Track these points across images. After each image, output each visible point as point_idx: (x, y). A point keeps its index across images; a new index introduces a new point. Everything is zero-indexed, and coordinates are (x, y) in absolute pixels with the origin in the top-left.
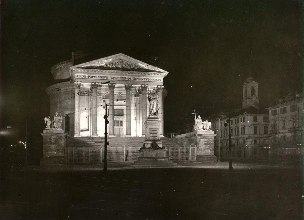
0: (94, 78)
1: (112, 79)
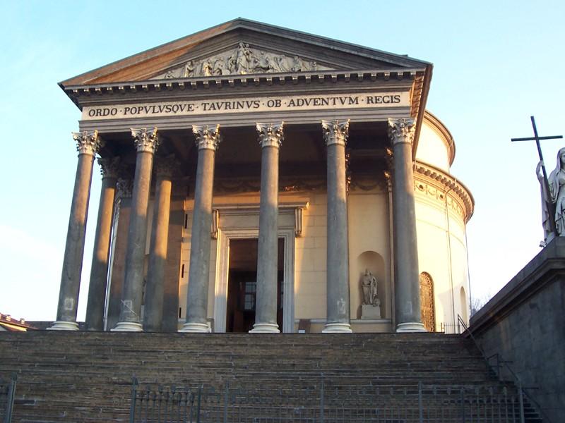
0: (143, 114)
1: (205, 113)
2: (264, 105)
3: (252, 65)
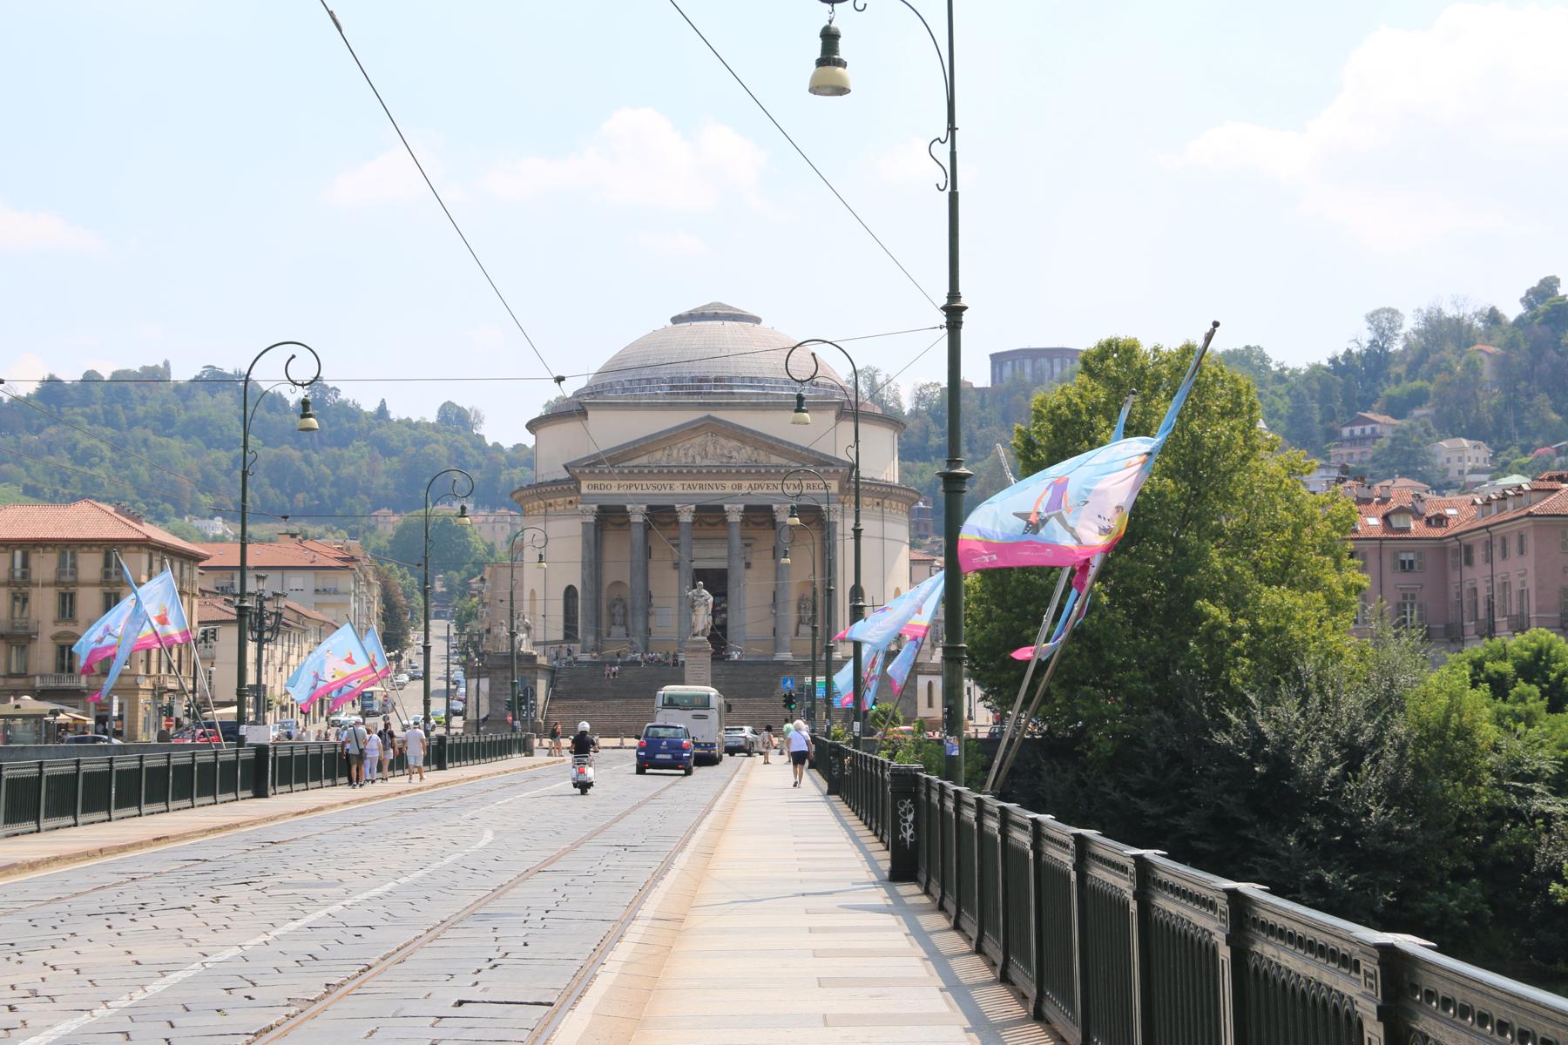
0: (633, 490)
2: (729, 486)
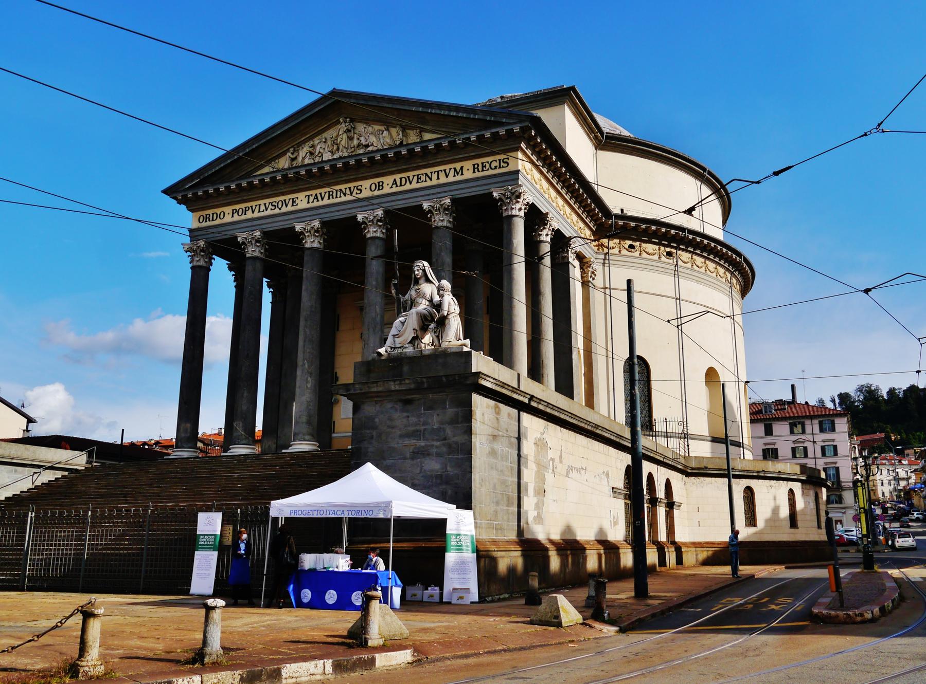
0: (249, 215)
3: (355, 142)
